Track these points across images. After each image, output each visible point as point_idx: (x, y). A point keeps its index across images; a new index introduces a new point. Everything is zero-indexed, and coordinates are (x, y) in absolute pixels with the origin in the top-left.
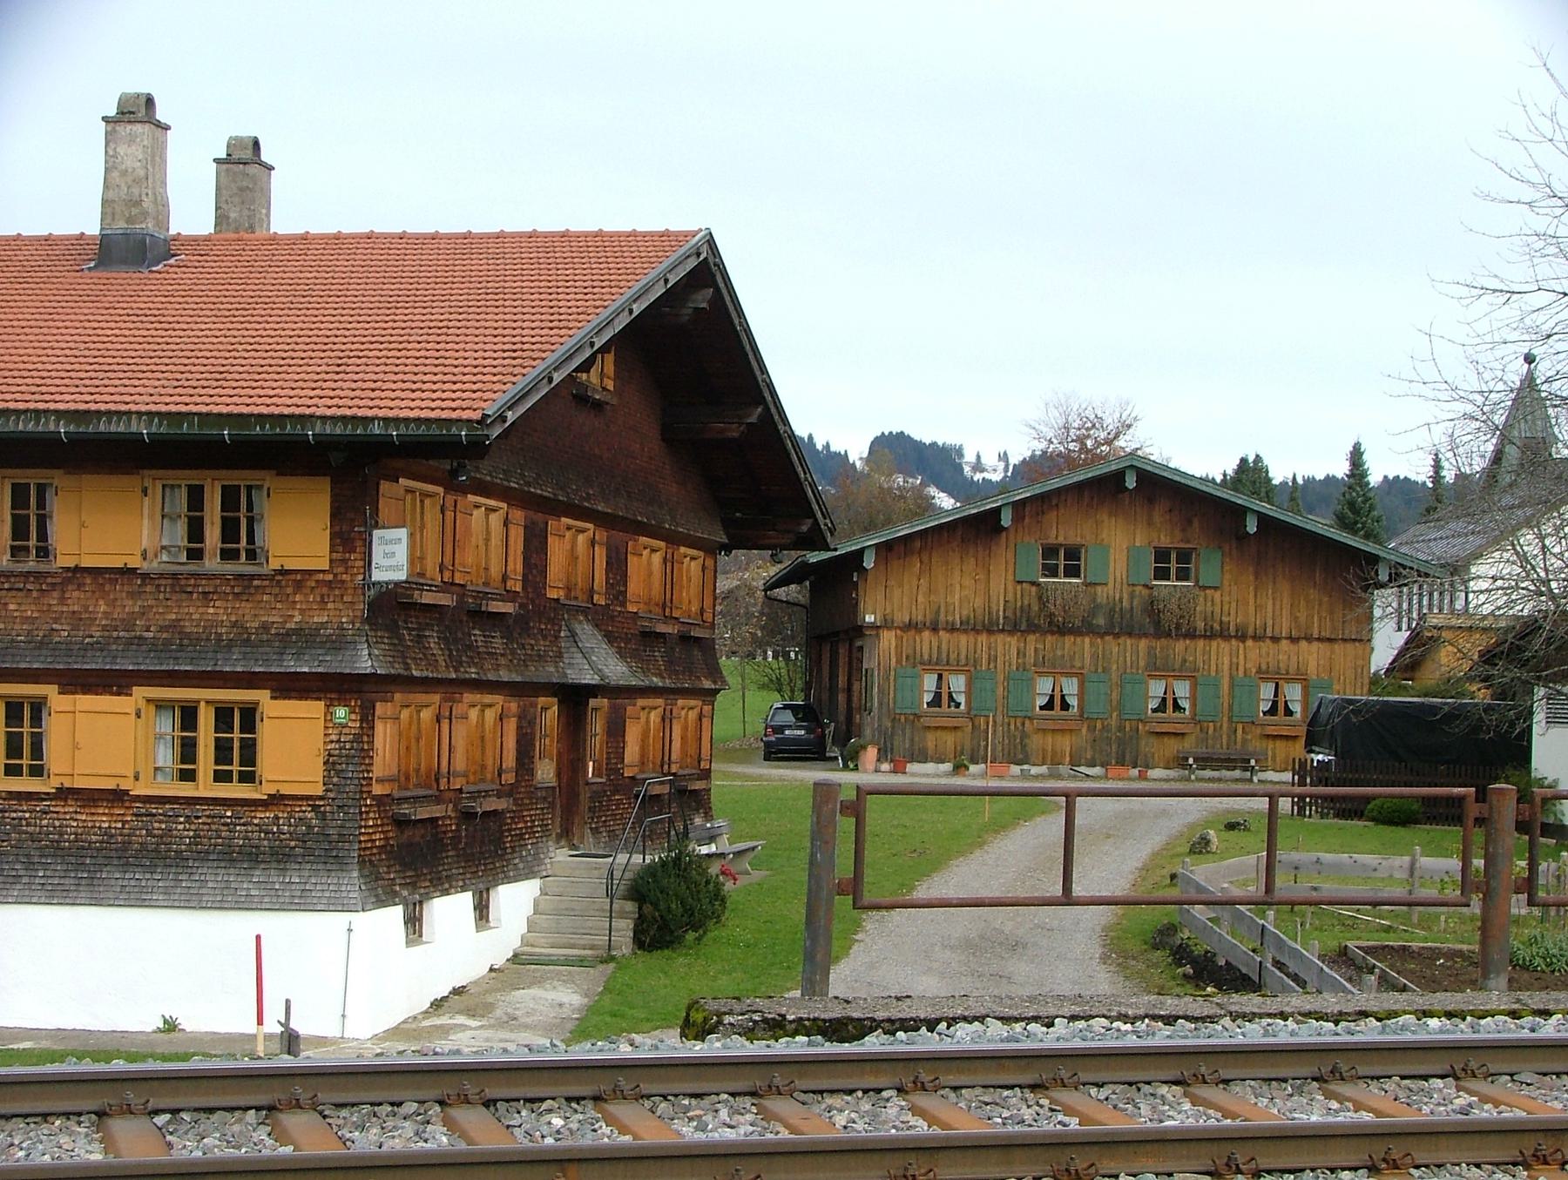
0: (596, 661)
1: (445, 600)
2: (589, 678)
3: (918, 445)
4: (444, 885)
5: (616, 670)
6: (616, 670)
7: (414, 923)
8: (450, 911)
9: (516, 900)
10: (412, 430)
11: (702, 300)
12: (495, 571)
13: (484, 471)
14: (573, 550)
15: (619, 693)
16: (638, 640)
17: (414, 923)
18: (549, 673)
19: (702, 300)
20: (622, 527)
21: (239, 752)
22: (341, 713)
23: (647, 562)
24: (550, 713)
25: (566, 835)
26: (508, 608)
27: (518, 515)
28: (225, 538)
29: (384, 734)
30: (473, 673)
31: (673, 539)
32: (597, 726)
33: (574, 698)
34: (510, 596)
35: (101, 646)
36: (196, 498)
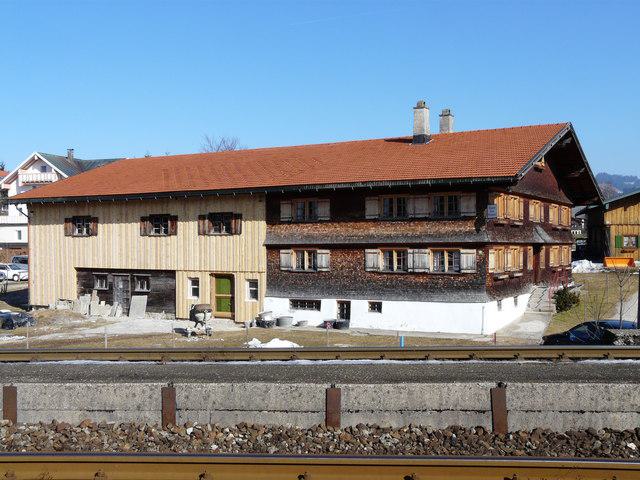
0: (543, 237)
1: (505, 222)
2: (541, 241)
3: (609, 176)
4: (506, 295)
5: (548, 239)
6: (548, 239)
7: (499, 305)
8: (508, 301)
9: (524, 298)
10: (375, 184)
11: (568, 141)
12: (516, 214)
13: (513, 189)
14: (536, 211)
15: (546, 244)
16: (551, 230)
17: (499, 305)
18: (530, 240)
19: (568, 141)
20: (547, 201)
21: (455, 261)
22: (480, 252)
23: (553, 211)
24: (531, 250)
25: (536, 283)
26: (521, 224)
27: (522, 200)
28: (450, 209)
29: (492, 259)
30: (512, 241)
31: (560, 204)
32: (542, 253)
33: (537, 247)
34: (521, 221)
35: (419, 237)
36: (391, 201)
